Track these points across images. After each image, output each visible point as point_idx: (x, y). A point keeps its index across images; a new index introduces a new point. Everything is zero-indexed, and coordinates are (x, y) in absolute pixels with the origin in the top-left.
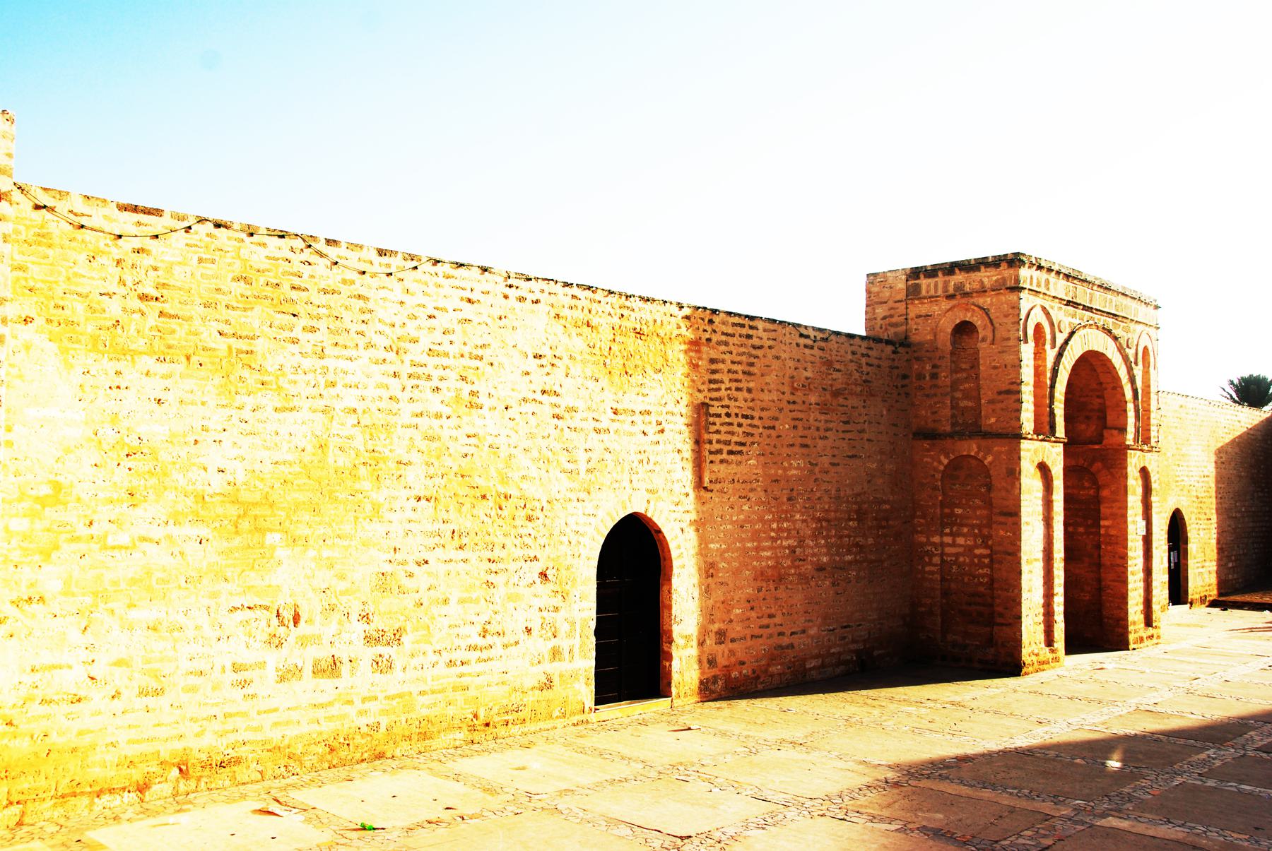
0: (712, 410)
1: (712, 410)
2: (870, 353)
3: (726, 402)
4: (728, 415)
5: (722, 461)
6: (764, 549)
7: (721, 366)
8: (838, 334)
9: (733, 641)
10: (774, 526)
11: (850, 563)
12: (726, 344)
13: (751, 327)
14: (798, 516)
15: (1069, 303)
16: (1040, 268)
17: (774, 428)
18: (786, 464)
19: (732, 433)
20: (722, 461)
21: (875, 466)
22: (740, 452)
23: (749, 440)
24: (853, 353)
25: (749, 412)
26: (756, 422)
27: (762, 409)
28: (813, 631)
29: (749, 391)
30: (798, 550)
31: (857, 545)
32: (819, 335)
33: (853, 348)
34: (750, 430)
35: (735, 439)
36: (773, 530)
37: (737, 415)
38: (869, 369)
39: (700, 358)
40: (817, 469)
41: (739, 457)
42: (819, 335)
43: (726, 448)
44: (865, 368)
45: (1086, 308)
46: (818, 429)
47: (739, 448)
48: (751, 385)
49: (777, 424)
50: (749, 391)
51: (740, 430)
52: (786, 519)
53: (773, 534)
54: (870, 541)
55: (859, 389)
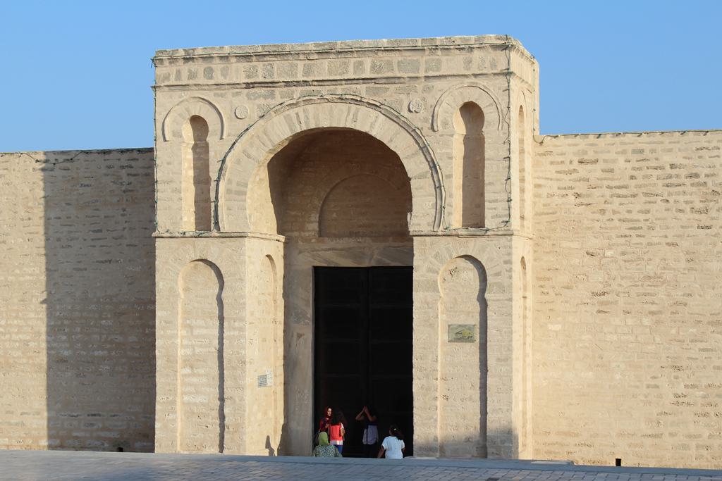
2: (133, 163)
8: (87, 152)
14: (32, 315)
15: (249, 86)
18: (18, 271)
21: (138, 269)
30: (31, 344)
32: (61, 158)
33: (109, 163)
38: (132, 179)
42: (61, 158)
44: (125, 179)
45: (287, 84)
46: (59, 240)
52: (16, 317)
54: (132, 338)
55: (115, 200)
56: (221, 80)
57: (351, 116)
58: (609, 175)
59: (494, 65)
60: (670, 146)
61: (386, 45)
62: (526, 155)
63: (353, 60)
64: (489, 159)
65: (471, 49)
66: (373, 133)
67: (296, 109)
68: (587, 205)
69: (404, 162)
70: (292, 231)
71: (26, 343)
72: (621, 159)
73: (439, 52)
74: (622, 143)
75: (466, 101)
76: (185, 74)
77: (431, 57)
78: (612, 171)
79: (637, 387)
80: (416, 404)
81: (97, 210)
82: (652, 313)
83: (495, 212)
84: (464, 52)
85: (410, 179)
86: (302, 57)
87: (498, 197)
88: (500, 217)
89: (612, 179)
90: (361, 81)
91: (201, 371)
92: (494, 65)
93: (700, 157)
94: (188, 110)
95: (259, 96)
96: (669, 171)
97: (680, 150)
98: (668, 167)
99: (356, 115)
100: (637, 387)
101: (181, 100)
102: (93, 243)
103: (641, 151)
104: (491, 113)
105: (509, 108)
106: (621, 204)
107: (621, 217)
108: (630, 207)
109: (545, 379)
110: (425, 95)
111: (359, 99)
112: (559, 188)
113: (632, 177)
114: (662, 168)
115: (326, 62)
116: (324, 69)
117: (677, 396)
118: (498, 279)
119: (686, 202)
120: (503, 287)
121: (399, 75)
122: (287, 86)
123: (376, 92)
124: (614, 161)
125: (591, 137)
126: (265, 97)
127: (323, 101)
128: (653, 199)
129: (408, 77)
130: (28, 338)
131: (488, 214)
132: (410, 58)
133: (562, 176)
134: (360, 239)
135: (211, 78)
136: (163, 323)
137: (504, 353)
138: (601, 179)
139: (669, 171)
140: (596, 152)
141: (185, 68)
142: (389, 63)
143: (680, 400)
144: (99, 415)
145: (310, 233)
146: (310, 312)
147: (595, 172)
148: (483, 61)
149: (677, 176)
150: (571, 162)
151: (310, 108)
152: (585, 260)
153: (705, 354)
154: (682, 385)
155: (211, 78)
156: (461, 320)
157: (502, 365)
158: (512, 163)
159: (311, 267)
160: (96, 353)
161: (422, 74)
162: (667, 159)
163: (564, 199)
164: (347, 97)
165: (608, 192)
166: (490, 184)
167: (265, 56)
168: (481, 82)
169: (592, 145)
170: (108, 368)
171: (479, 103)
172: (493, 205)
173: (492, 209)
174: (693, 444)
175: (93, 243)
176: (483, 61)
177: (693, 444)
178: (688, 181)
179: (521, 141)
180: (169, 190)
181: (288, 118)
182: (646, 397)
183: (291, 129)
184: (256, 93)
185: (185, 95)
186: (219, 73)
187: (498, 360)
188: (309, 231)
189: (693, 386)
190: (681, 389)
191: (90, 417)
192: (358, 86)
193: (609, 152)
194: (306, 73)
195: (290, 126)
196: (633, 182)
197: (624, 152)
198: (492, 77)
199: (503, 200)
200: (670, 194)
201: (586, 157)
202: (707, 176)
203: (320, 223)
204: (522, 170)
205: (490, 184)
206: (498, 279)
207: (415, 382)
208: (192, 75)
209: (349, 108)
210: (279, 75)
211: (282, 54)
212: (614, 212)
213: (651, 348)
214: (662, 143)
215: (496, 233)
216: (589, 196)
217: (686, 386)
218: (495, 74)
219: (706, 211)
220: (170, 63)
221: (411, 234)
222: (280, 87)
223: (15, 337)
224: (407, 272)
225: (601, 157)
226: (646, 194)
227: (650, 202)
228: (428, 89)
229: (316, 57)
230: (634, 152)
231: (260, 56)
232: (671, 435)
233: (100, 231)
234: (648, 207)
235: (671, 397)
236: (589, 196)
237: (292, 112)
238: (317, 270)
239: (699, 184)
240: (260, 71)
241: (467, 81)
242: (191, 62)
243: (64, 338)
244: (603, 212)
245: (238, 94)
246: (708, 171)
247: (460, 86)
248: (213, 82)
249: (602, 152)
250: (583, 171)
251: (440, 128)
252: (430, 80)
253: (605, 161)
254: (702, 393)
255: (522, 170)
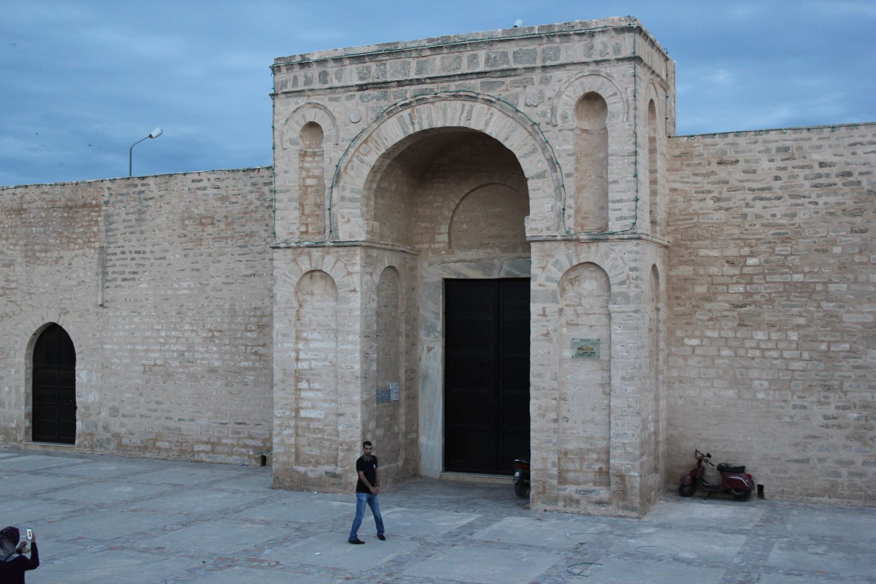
0: (110, 251)
1: (110, 251)
3: (121, 243)
4: (123, 253)
5: (116, 287)
6: (153, 351)
7: (116, 218)
9: (124, 416)
10: (163, 334)
11: (248, 369)
12: (121, 201)
13: (143, 185)
14: (187, 327)
15: (361, 88)
16: (304, 64)
17: (165, 258)
18: (176, 286)
19: (126, 266)
20: (116, 287)
22: (133, 279)
23: (140, 270)
24: (254, 184)
25: (141, 249)
26: (147, 255)
27: (154, 245)
28: (204, 422)
29: (142, 232)
30: (186, 354)
31: (256, 353)
33: (253, 180)
34: (143, 262)
35: (128, 270)
36: (161, 337)
37: (131, 252)
39: (99, 216)
40: (208, 289)
41: (131, 283)
43: (120, 277)
45: (400, 83)
47: (132, 276)
48: (143, 228)
49: (167, 255)
50: (142, 232)
51: (133, 263)
52: (175, 329)
53: (161, 340)
56: (336, 83)
57: (465, 112)
58: (750, 176)
59: (617, 50)
60: (819, 143)
61: (500, 35)
62: (658, 156)
63: (466, 55)
64: (612, 155)
65: (592, 34)
66: (488, 132)
67: (409, 111)
68: (727, 209)
69: (522, 161)
70: (423, 243)
71: (182, 354)
72: (764, 159)
73: (557, 40)
74: (765, 141)
75: (587, 91)
76: (301, 80)
77: (549, 45)
78: (754, 172)
79: (782, 407)
80: (533, 426)
81: (243, 226)
82: (799, 327)
83: (618, 214)
84: (585, 38)
85: (526, 180)
86: (414, 54)
87: (623, 196)
88: (625, 219)
89: (753, 181)
90: (475, 76)
91: (317, 386)
92: (617, 50)
93: (854, 154)
94: (304, 117)
95: (373, 98)
96: (818, 170)
97: (830, 146)
98: (816, 165)
99: (470, 113)
100: (782, 407)
101: (297, 106)
102: (239, 258)
103: (786, 149)
104: (615, 103)
105: (635, 96)
106: (764, 208)
107: (765, 221)
108: (774, 211)
109: (681, 397)
110: (542, 87)
111: (474, 95)
112: (696, 192)
113: (777, 178)
114: (808, 167)
115: (438, 57)
116: (437, 65)
117: (826, 417)
118: (624, 288)
119: (838, 204)
120: (629, 297)
121: (514, 67)
122: (398, 86)
123: (491, 86)
124: (757, 161)
125: (731, 136)
126: (378, 99)
127: (435, 99)
128: (800, 201)
129: (524, 68)
130: (184, 349)
131: (612, 215)
132: (525, 48)
133: (699, 179)
134: (489, 251)
135: (326, 82)
136: (280, 336)
137: (630, 371)
138: (743, 181)
139: (818, 170)
140: (736, 152)
141: (300, 73)
142: (505, 55)
143: (831, 422)
144: (245, 424)
145: (440, 245)
146: (440, 325)
147: (735, 175)
148: (605, 45)
149: (828, 175)
150: (709, 164)
151: (421, 107)
152: (725, 269)
153: (859, 372)
154: (833, 406)
155: (326, 82)
156: (584, 333)
157: (627, 385)
158: (639, 158)
159: (441, 279)
160: (242, 364)
161: (539, 64)
162: (817, 157)
163: (701, 203)
164: (461, 93)
165: (750, 196)
166: (614, 182)
167: (377, 55)
168: (604, 69)
169: (732, 144)
170: (252, 378)
171: (600, 92)
172: (617, 206)
173: (616, 210)
174: (844, 471)
175: (239, 258)
176: (605, 45)
177: (844, 471)
178: (839, 181)
179: (652, 140)
180: (286, 200)
181: (401, 119)
182: (792, 418)
183: (404, 132)
184: (369, 95)
185: (302, 101)
186: (334, 77)
187: (623, 378)
188: (439, 243)
189: (845, 408)
190: (831, 410)
191: (238, 426)
192: (473, 82)
193: (750, 151)
194: (419, 72)
195: (403, 128)
196: (779, 183)
197: (768, 151)
198: (615, 63)
199: (628, 200)
200: (819, 196)
201: (725, 158)
202: (861, 174)
203: (449, 234)
204: (653, 171)
205: (614, 182)
206: (624, 288)
207: (532, 402)
208: (308, 81)
209: (464, 106)
210: (392, 75)
211: (393, 52)
212: (758, 217)
213: (799, 365)
214: (810, 139)
215: (621, 236)
216: (729, 199)
217: (837, 407)
218: (618, 60)
219: (858, 212)
220: (288, 69)
221: (527, 239)
222: (393, 87)
223: (174, 348)
224: (525, 282)
225: (741, 157)
226: (792, 196)
227: (797, 205)
228: (545, 81)
229: (428, 53)
230: (779, 150)
231: (373, 56)
232: (820, 460)
233: (246, 246)
234: (794, 209)
235: (820, 418)
236: (729, 199)
237: (405, 113)
238: (447, 282)
239: (852, 183)
240: (374, 71)
241: (587, 70)
242: (306, 68)
243: (215, 349)
244: (745, 216)
245: (352, 97)
246: (863, 169)
247: (581, 75)
248: (327, 86)
249: (743, 152)
250: (723, 173)
251: (559, 122)
252: (548, 70)
253: (747, 161)
254: (855, 415)
255: (653, 171)
